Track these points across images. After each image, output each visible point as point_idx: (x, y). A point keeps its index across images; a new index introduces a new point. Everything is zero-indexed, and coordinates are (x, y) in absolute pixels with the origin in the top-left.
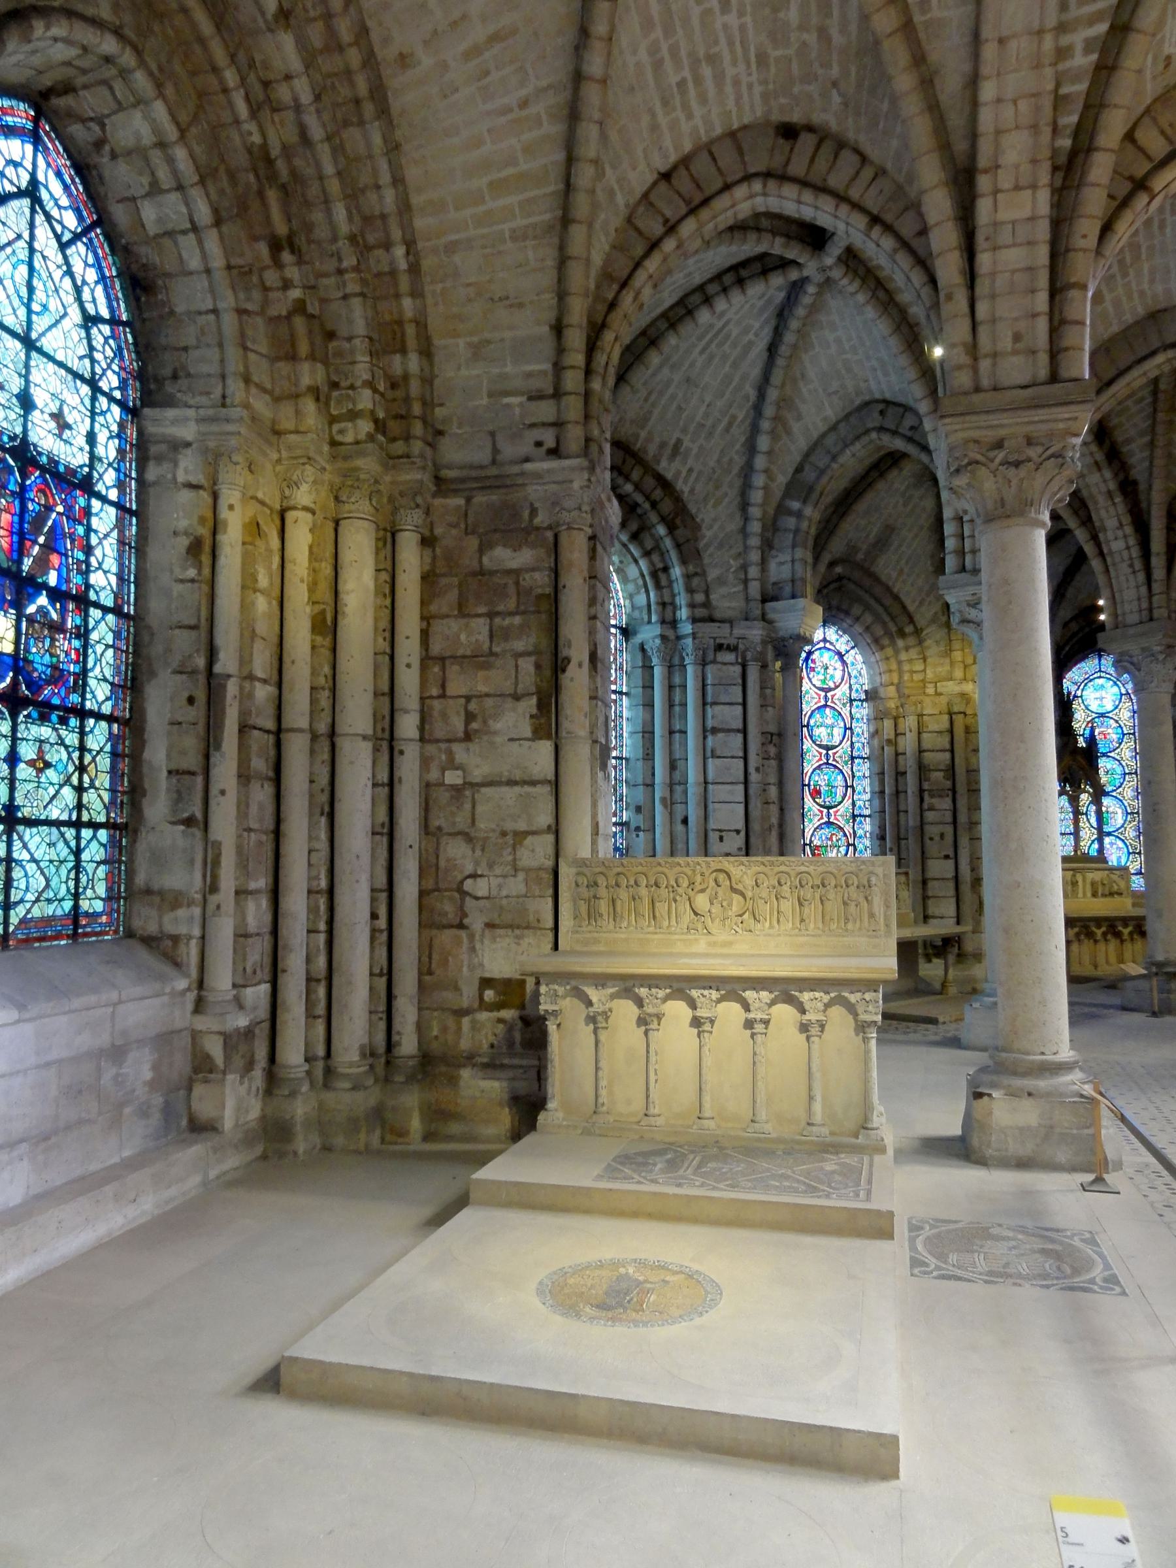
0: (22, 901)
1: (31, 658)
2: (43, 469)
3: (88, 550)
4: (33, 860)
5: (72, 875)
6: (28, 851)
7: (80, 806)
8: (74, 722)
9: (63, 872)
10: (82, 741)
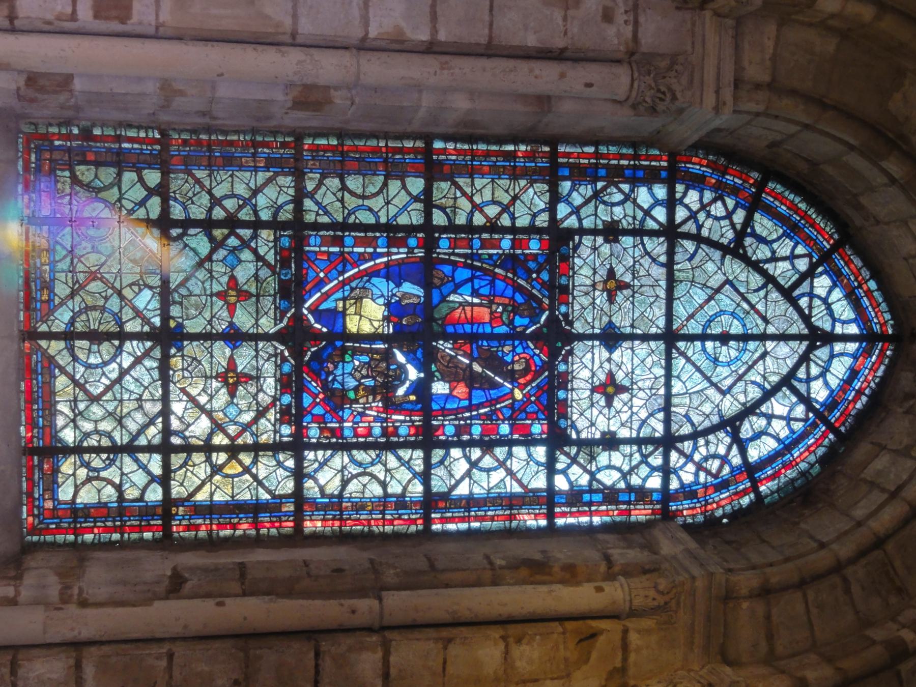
0: (75, 359)
1: (348, 358)
2: (550, 366)
3: (487, 446)
4: (123, 373)
5: (105, 442)
6: (133, 366)
7: (188, 449)
8: (286, 430)
9: (106, 426)
10: (266, 447)
